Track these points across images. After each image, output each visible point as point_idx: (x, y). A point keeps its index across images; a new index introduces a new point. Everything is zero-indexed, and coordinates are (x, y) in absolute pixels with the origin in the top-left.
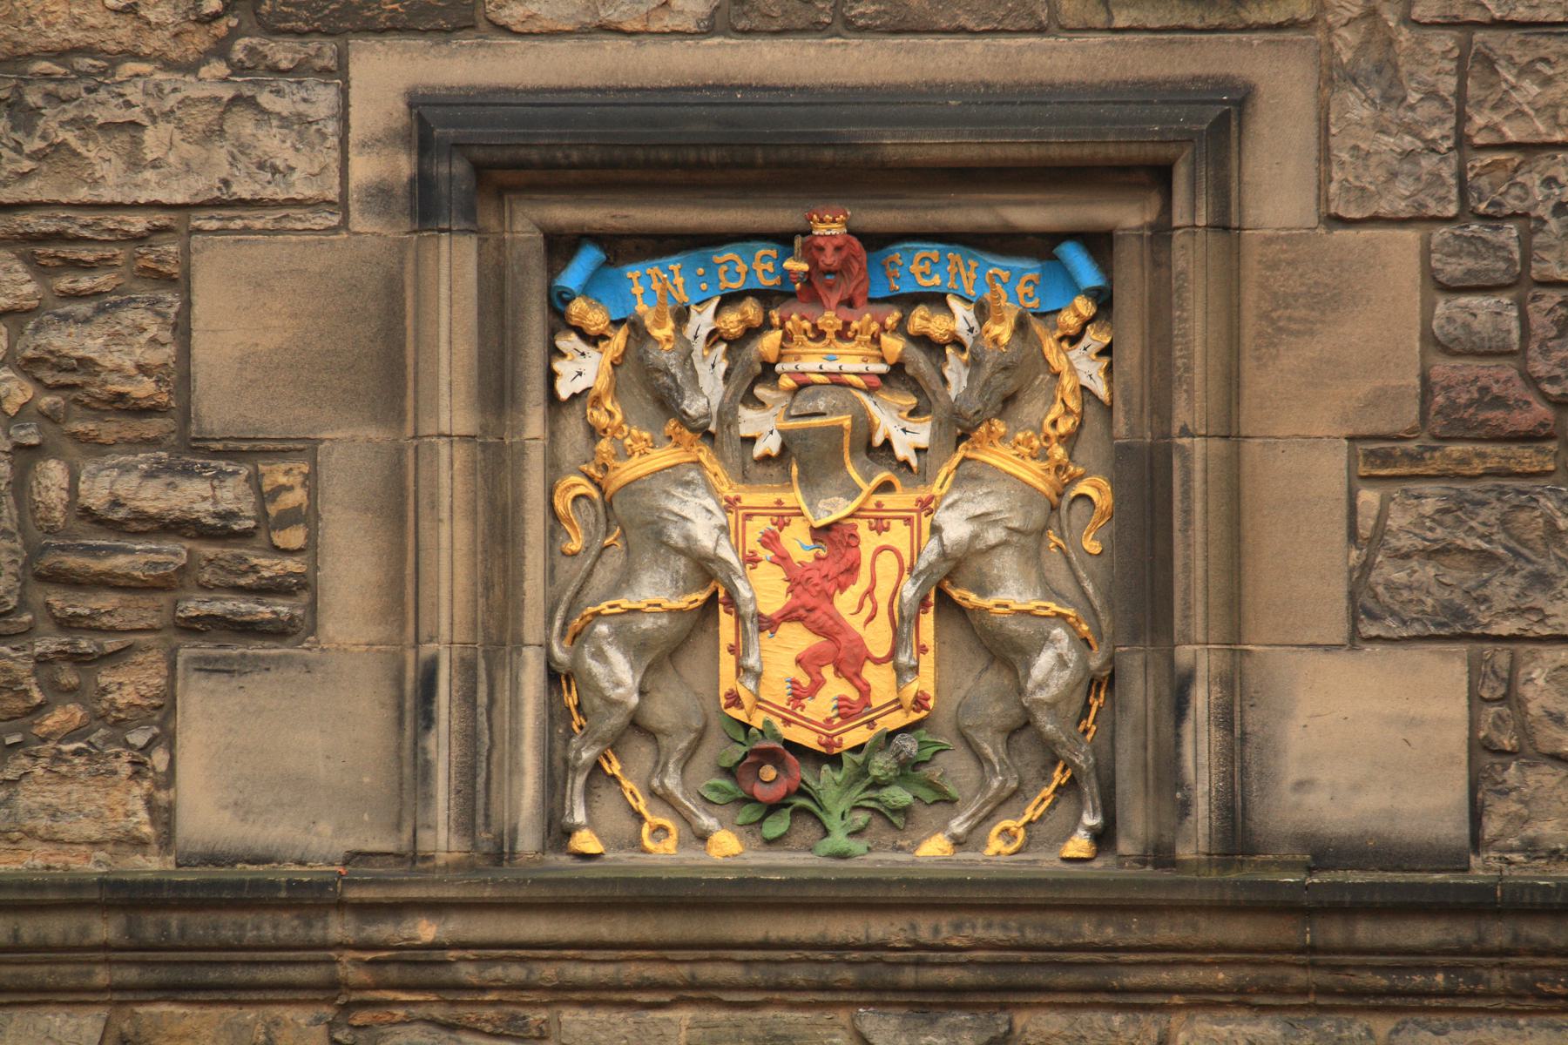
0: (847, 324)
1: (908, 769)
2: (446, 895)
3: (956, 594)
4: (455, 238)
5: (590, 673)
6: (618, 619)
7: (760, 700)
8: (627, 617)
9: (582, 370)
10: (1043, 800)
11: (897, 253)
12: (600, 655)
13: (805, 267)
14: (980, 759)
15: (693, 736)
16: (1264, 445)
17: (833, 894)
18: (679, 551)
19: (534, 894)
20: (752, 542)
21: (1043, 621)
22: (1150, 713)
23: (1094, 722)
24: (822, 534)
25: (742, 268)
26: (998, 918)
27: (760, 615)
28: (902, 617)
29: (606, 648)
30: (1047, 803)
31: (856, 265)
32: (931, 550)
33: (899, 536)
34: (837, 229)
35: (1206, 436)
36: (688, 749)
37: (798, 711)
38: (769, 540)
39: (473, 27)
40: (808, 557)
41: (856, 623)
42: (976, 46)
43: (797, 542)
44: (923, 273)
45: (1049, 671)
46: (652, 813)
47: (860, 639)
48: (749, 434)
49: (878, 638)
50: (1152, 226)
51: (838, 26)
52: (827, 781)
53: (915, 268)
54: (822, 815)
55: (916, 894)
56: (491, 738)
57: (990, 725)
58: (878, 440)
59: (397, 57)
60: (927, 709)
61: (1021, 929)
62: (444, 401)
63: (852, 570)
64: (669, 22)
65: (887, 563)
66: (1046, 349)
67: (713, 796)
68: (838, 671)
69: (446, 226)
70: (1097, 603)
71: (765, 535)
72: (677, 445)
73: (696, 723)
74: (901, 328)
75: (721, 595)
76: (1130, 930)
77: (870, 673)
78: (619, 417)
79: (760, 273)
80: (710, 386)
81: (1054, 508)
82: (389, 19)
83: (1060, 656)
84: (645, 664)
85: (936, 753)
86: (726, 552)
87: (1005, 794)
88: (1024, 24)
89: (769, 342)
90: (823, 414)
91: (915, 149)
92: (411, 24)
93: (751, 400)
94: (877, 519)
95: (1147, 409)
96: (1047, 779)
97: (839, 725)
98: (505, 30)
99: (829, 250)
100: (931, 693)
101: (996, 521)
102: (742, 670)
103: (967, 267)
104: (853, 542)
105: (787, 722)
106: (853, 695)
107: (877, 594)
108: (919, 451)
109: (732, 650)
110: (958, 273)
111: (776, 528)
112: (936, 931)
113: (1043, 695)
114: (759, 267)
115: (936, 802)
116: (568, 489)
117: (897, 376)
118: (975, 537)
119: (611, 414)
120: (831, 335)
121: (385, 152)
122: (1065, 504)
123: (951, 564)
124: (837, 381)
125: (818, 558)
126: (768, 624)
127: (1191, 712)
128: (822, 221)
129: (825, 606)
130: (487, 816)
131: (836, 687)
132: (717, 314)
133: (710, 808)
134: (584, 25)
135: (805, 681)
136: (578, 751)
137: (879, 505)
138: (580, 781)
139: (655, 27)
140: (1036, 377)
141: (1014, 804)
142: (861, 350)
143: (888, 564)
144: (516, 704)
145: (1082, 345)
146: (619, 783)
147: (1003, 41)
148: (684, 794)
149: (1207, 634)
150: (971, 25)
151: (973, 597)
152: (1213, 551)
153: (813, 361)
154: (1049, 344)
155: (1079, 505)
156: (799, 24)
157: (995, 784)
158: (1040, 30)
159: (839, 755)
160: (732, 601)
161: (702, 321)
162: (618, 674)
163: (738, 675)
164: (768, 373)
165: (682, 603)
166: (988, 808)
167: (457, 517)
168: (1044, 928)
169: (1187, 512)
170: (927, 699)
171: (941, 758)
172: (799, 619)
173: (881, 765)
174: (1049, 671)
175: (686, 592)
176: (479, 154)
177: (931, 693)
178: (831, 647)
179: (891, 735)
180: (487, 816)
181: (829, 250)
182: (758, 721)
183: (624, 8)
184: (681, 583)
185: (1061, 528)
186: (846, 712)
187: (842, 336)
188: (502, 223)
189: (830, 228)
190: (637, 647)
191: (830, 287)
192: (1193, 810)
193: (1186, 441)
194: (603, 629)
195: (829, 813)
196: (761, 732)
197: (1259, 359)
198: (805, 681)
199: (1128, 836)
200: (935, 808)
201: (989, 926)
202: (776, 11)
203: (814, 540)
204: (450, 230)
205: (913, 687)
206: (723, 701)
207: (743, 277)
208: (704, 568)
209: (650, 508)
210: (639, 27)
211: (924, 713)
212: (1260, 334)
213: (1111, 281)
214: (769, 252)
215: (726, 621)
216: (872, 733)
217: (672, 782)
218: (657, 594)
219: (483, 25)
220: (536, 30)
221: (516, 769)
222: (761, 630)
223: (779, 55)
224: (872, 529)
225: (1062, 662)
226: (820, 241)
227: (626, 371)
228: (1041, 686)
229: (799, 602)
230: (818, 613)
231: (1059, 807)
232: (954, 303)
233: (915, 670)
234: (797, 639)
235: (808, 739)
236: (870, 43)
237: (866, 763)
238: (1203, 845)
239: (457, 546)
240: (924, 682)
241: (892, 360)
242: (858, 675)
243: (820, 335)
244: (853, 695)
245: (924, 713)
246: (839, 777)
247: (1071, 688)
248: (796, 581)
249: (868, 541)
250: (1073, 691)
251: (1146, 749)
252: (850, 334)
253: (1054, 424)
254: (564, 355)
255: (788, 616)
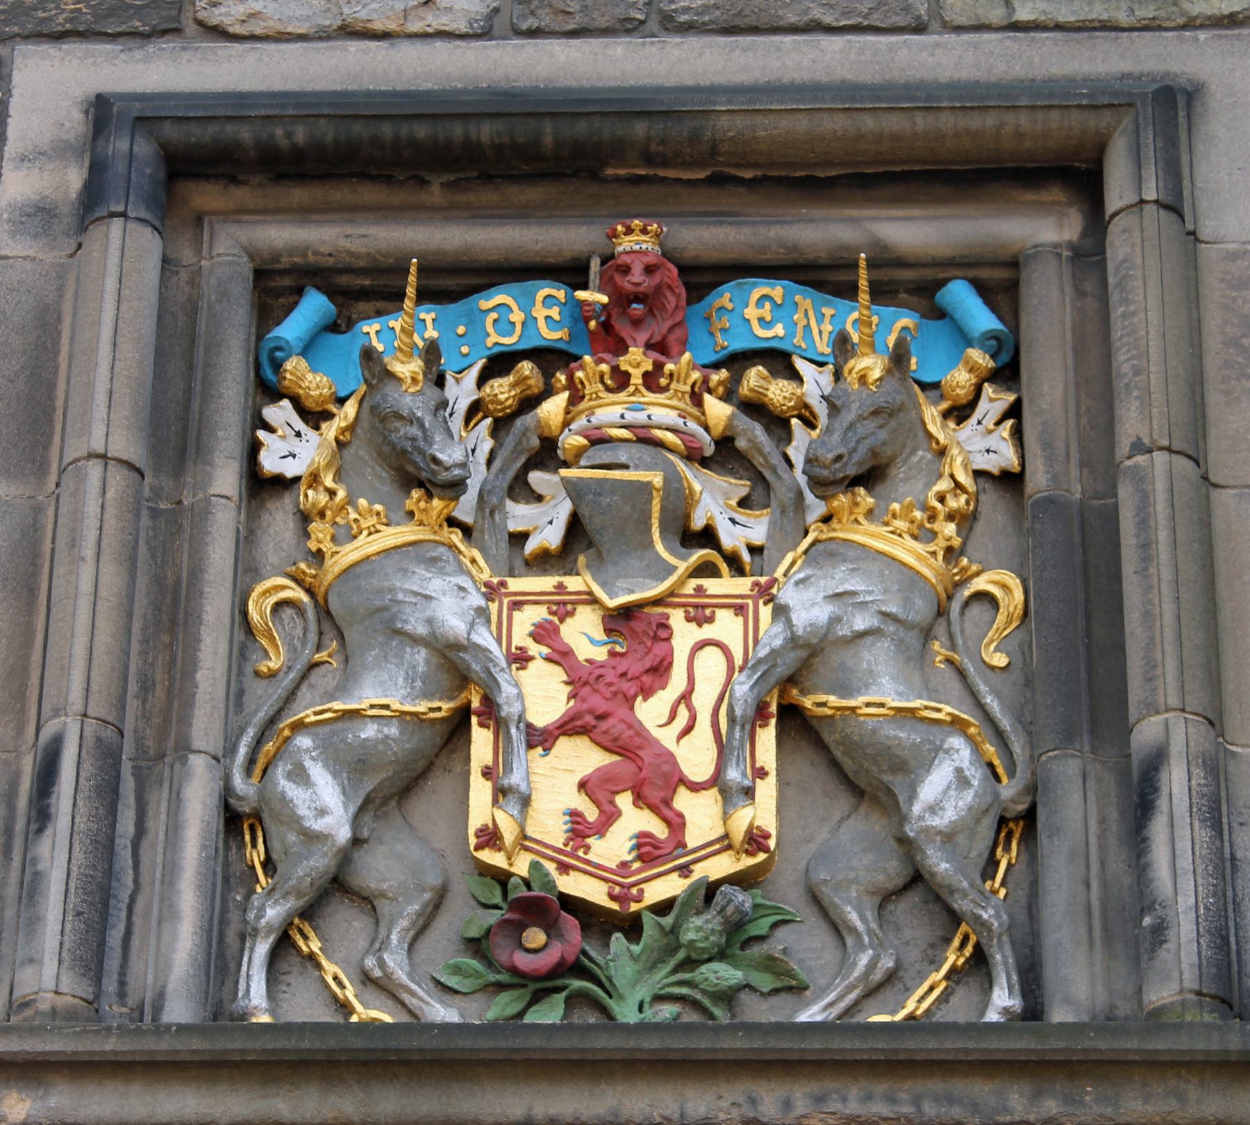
0: (659, 366)
1: (737, 938)
2: (48, 1047)
3: (808, 702)
4: (131, 225)
5: (283, 794)
6: (327, 729)
7: (525, 837)
8: (339, 725)
9: (291, 450)
10: (931, 989)
11: (725, 296)
12: (300, 775)
13: (604, 299)
14: (837, 928)
15: (427, 896)
16: (1241, 496)
17: (632, 1044)
18: (416, 640)
19: (180, 1047)
20: (521, 636)
21: (934, 729)
22: (1093, 840)
23: (1003, 884)
24: (621, 620)
25: (517, 316)
26: (881, 1087)
27: (529, 726)
28: (732, 720)
29: (308, 764)
30: (936, 993)
31: (672, 299)
32: (772, 634)
33: (727, 627)
34: (646, 244)
35: (1169, 449)
36: (419, 915)
37: (580, 853)
38: (543, 633)
39: (177, 31)
40: (600, 654)
41: (667, 737)
42: (836, 43)
43: (584, 635)
44: (761, 320)
45: (945, 792)
46: (366, 1006)
47: (671, 756)
48: (520, 528)
49: (696, 756)
50: (1071, 246)
51: (653, 25)
52: (619, 956)
53: (751, 312)
54: (611, 1003)
55: (758, 1044)
56: (136, 881)
57: (856, 881)
58: (698, 523)
59: (75, 62)
60: (766, 850)
61: (917, 1101)
62: (100, 410)
63: (661, 670)
64: (432, 20)
65: (711, 667)
66: (928, 419)
67: (453, 982)
68: (640, 799)
69: (121, 208)
70: (1005, 723)
71: (538, 626)
72: (421, 524)
73: (433, 879)
74: (727, 397)
75: (475, 704)
76: (1082, 1103)
77: (684, 801)
78: (341, 494)
79: (541, 323)
80: (466, 449)
81: (941, 612)
82: (70, 20)
83: (959, 771)
84: (362, 794)
85: (775, 925)
86: (484, 638)
87: (878, 976)
88: (900, 20)
89: (552, 409)
90: (625, 467)
91: (759, 120)
92: (98, 28)
93: (520, 489)
94: (696, 606)
95: (1075, 456)
96: (935, 963)
97: (639, 871)
98: (219, 33)
99: (637, 269)
100: (773, 831)
101: (866, 603)
102: (501, 793)
103: (821, 318)
104: (663, 634)
105: (564, 868)
106: (659, 830)
107: (696, 700)
108: (755, 550)
109: (487, 773)
110: (807, 327)
111: (555, 619)
112: (787, 1105)
113: (935, 822)
114: (540, 312)
115: (776, 991)
116: (267, 593)
117: (725, 454)
118: (835, 620)
119: (332, 493)
120: (637, 379)
121: (50, 166)
122: (955, 607)
123: (803, 654)
124: (645, 438)
125: (612, 654)
126: (541, 739)
127: (1162, 803)
128: (629, 231)
129: (622, 712)
130: (122, 983)
131: (635, 820)
132: (482, 381)
133: (448, 997)
134: (323, 29)
135: (591, 814)
136: (262, 909)
137: (699, 590)
138: (262, 948)
139: (414, 27)
140: (913, 452)
141: (888, 994)
142: (674, 402)
143: (711, 657)
144: (174, 829)
145: (973, 420)
146: (318, 966)
147: (871, 38)
148: (410, 976)
149: (1183, 698)
150: (828, 19)
151: (833, 700)
152: (1185, 595)
153: (610, 412)
154: (931, 414)
155: (976, 610)
156: (603, 22)
157: (864, 959)
158: (920, 29)
159: (637, 916)
160: (491, 712)
161: (462, 392)
162: (322, 801)
163: (495, 802)
164: (547, 454)
165: (422, 707)
166: (853, 996)
167: (105, 558)
168: (951, 1100)
169: (1146, 546)
170: (767, 836)
171: (782, 932)
172: (584, 731)
173: (700, 929)
174: (945, 792)
175: (427, 695)
176: (170, 132)
177: (773, 831)
178: (629, 768)
179: (711, 890)
180: (122, 983)
181: (637, 269)
182: (522, 866)
183: (375, 6)
184: (418, 684)
185: (951, 637)
186: (647, 851)
187: (651, 381)
188: (199, 250)
189: (636, 243)
190: (352, 765)
191: (637, 323)
192: (1171, 934)
193: (1140, 459)
194: (304, 741)
195: (621, 998)
196: (527, 883)
197: (1227, 393)
198: (591, 814)
199: (1068, 1001)
200: (774, 1000)
201: (869, 1097)
202: (574, 7)
203: (608, 631)
204: (123, 215)
205: (743, 818)
206: (473, 841)
207: (518, 327)
208: (454, 665)
209: (380, 591)
210: (392, 26)
211: (762, 857)
212: (1227, 364)
213: (1015, 329)
214: (553, 292)
215: (481, 741)
216: (685, 883)
217: (396, 963)
218: (388, 693)
219: (191, 28)
220: (258, 31)
221: (169, 912)
222: (530, 746)
223: (576, 55)
224: (689, 619)
225: (962, 780)
226: (627, 259)
227: (360, 450)
228: (933, 809)
229: (585, 706)
230: (611, 721)
231: (954, 1000)
232: (800, 365)
233: (749, 793)
234: (581, 757)
235: (593, 891)
236: (694, 42)
237: (674, 930)
238: (1190, 979)
239: (103, 593)
240: (763, 811)
241: (718, 430)
242: (668, 802)
243: (621, 380)
244: (659, 830)
245: (762, 857)
246: (636, 949)
247: (975, 814)
248: (581, 680)
249: (684, 634)
250: (978, 821)
251: (1088, 885)
252: (663, 382)
253: (942, 499)
254: (271, 429)
255: (568, 727)
